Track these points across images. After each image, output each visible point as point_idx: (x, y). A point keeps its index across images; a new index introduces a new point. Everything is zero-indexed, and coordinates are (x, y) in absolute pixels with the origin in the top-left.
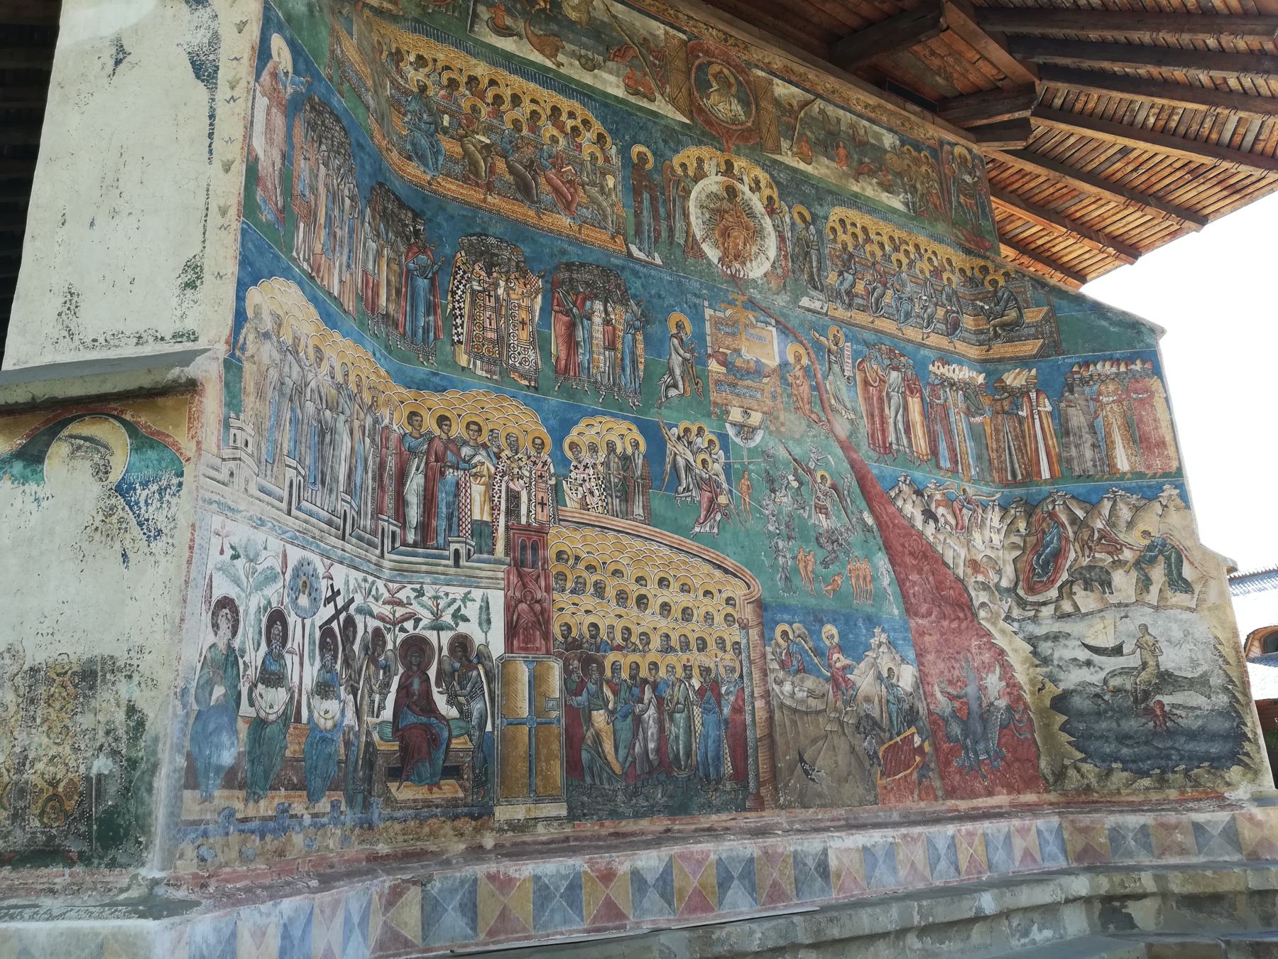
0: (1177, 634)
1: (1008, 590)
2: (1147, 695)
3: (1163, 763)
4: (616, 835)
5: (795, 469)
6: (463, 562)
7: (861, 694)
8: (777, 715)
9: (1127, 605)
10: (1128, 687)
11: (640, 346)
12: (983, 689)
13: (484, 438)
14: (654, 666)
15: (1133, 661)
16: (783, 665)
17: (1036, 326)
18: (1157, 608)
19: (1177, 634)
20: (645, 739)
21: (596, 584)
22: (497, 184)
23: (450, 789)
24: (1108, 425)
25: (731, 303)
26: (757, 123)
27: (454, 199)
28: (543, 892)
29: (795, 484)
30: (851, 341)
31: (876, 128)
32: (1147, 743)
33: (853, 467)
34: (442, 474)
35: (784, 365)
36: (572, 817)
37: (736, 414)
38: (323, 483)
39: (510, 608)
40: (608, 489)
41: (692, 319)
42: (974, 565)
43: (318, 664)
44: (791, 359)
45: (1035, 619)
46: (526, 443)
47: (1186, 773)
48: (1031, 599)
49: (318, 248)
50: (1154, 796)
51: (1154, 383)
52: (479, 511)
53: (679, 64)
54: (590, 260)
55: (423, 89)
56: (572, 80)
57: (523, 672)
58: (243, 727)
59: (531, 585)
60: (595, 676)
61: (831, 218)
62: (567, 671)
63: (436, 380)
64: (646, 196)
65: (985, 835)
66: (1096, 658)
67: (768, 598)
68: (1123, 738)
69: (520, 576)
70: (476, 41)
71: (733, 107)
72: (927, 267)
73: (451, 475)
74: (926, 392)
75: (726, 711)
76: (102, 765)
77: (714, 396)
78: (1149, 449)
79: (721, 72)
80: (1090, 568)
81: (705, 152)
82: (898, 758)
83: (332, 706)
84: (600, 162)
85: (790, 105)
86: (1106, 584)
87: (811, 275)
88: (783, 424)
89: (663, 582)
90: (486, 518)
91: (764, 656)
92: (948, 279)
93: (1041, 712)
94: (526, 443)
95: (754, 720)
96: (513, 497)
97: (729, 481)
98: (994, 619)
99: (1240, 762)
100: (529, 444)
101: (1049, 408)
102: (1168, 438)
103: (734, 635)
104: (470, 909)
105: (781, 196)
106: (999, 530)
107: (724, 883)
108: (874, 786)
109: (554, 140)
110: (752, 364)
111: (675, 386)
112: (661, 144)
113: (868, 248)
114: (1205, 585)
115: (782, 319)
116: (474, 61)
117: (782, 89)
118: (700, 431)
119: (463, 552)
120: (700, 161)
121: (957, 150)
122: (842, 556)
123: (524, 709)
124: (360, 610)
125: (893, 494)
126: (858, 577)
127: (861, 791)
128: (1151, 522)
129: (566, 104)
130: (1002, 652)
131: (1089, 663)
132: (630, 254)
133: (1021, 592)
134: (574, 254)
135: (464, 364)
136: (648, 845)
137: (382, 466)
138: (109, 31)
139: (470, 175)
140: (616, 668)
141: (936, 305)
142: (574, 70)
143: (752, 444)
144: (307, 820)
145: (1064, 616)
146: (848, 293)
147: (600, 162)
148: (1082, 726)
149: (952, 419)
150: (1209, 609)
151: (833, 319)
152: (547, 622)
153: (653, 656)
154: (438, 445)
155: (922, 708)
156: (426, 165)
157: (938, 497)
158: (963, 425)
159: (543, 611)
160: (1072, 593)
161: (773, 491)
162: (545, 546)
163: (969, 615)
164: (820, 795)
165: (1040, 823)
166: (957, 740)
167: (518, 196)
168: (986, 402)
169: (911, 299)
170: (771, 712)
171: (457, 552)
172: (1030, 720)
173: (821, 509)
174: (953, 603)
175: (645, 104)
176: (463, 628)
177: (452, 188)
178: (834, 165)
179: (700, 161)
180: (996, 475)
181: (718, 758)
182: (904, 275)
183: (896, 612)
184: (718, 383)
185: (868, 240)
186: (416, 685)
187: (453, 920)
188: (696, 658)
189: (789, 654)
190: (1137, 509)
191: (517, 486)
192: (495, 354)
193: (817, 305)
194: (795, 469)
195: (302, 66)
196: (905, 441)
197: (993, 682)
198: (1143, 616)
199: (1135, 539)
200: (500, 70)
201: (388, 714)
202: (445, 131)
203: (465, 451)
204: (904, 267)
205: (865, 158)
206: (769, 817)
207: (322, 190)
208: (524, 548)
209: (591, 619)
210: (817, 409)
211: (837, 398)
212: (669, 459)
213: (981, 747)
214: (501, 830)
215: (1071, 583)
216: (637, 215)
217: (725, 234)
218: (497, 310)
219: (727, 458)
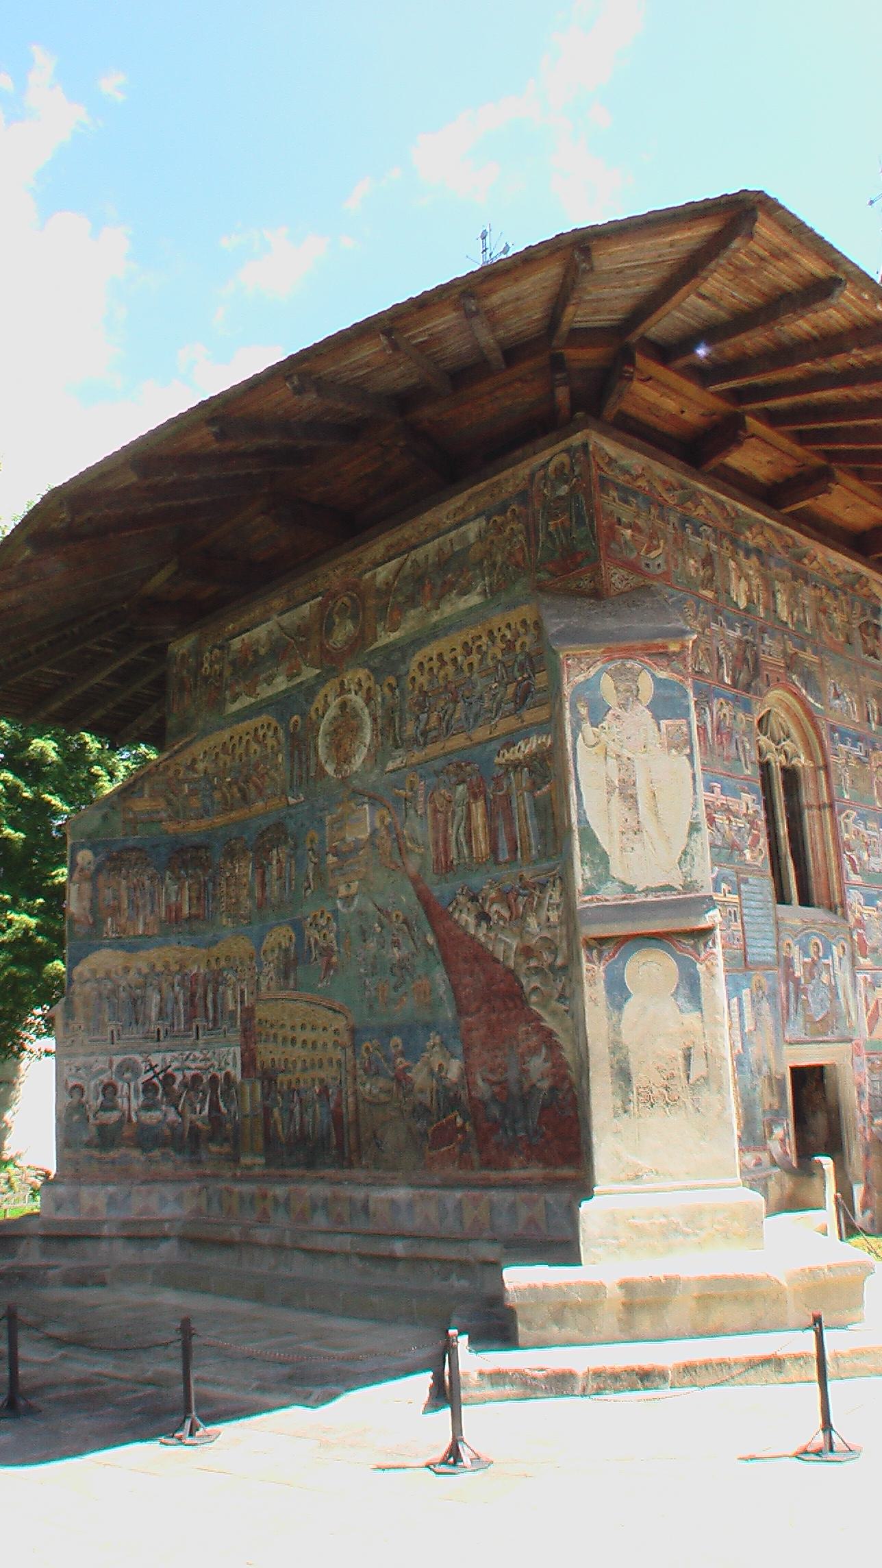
7: (417, 1086)
8: (361, 1107)
12: (524, 1072)
14: (298, 1080)
16: (365, 1070)
23: (226, 1148)
29: (379, 929)
37: (343, 891)
38: (137, 1023)
42: (527, 952)
43: (141, 1098)
44: (378, 824)
49: (123, 921)
52: (231, 1007)
57: (248, 1089)
62: (263, 1088)
65: (491, 1202)
73: (221, 988)
75: (332, 1105)
82: (443, 1136)
83: (156, 1115)
91: (355, 1066)
103: (338, 1054)
107: (314, 1208)
113: (442, 673)
117: (383, 574)
122: (408, 978)
124: (178, 1069)
130: (550, 1034)
137: (193, 995)
149: (515, 805)
153: (297, 1075)
155: (464, 1094)
157: (493, 894)
163: (519, 1003)
170: (357, 1105)
173: (396, 944)
177: (219, 820)
181: (329, 1134)
182: (475, 675)
185: (443, 663)
189: (370, 1063)
196: (466, 852)
197: (538, 1065)
201: (206, 1112)
207: (124, 893)
209: (271, 1056)
210: (396, 857)
211: (413, 840)
213: (519, 1125)
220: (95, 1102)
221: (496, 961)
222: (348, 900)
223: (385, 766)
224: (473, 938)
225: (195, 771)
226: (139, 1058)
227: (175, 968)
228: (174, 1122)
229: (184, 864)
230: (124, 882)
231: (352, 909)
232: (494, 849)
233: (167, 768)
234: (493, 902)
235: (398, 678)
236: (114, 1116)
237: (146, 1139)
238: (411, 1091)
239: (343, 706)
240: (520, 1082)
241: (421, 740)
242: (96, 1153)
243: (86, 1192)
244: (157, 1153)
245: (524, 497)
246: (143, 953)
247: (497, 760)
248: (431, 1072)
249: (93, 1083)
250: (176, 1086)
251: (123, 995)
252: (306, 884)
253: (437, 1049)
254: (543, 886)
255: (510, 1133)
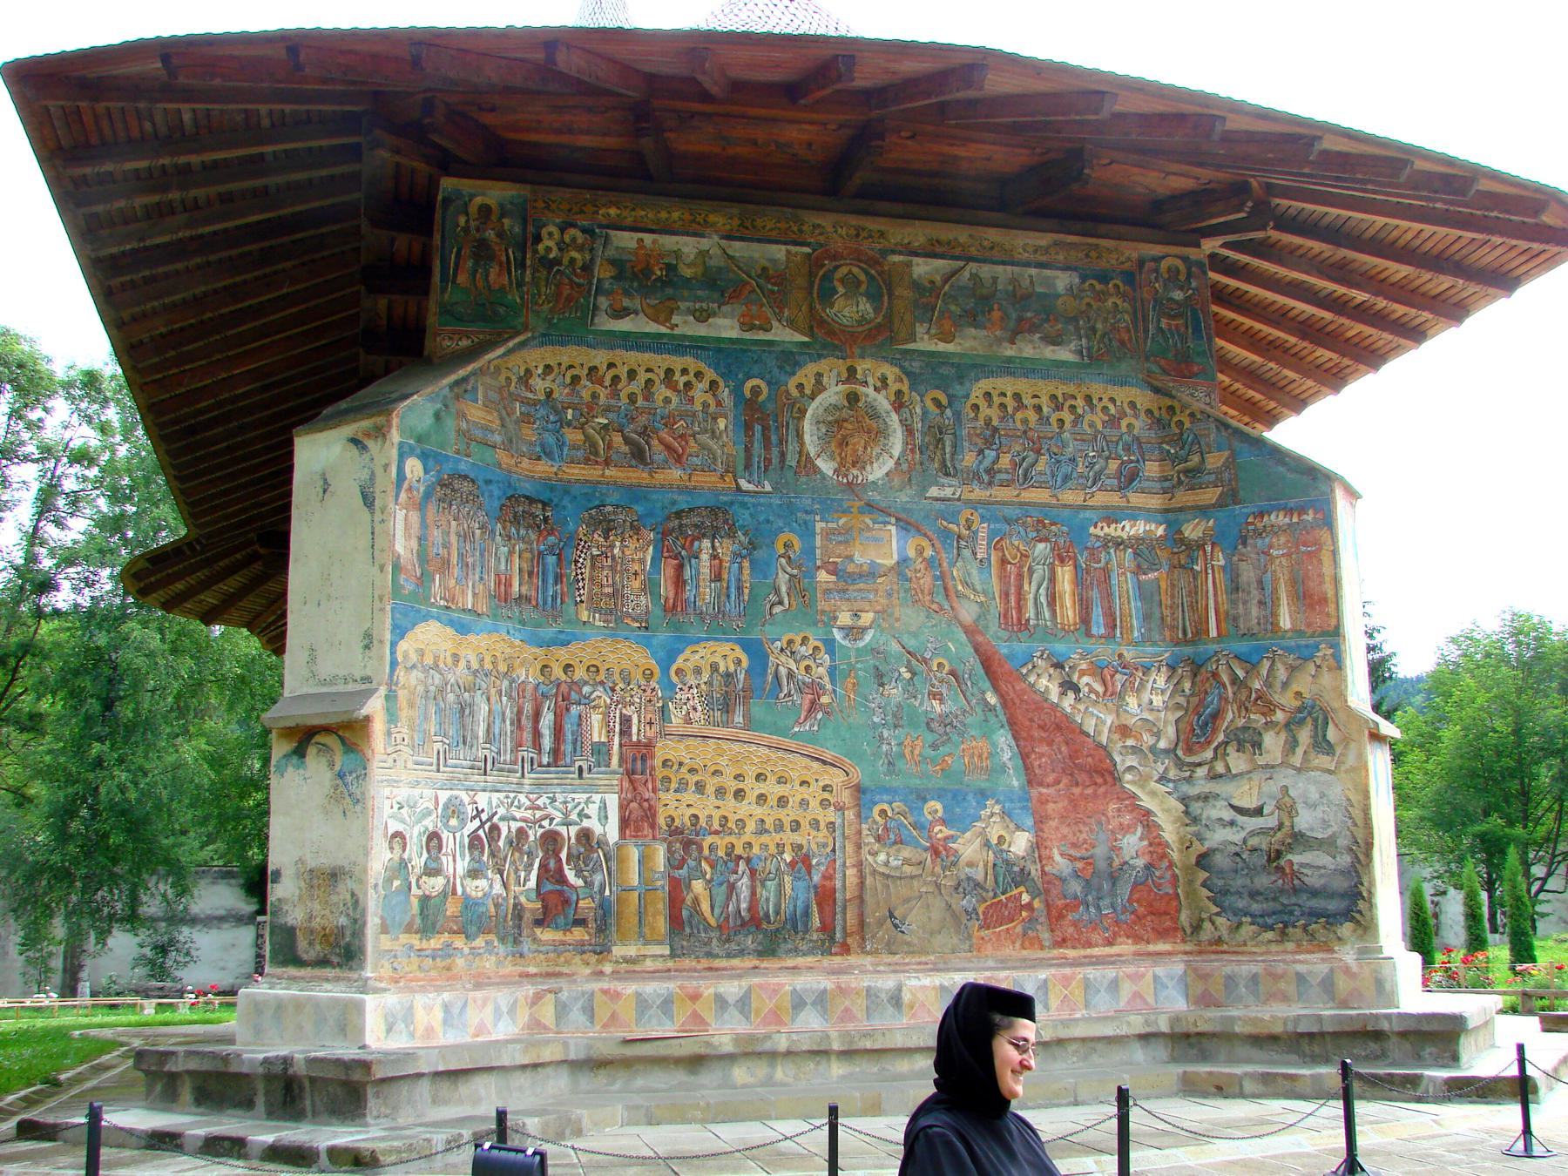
0: (1314, 796)
1: (1166, 751)
2: (1279, 854)
3: (1286, 918)
4: (710, 969)
5: (909, 661)
6: (585, 775)
8: (869, 881)
9: (1273, 767)
10: (1264, 847)
11: (746, 572)
13: (602, 677)
15: (1270, 822)
16: (878, 839)
17: (1218, 472)
18: (1299, 770)
19: (1314, 796)
20: (738, 901)
21: (697, 783)
22: (614, 457)
23: (578, 934)
24: (1275, 581)
25: (845, 512)
26: (889, 318)
27: (577, 481)
28: (642, 1003)
29: (907, 675)
30: (988, 521)
31: (1048, 272)
32: (1274, 899)
33: (976, 651)
34: (568, 710)
35: (904, 561)
36: (673, 955)
37: (845, 618)
39: (623, 807)
40: (709, 702)
41: (801, 537)
42: (1124, 731)
43: (468, 858)
44: (911, 553)
45: (1189, 780)
46: (637, 676)
47: (1305, 928)
48: (1188, 760)
49: (452, 583)
50: (1274, 948)
51: (1324, 535)
52: (598, 735)
53: (801, 281)
54: (699, 503)
55: (549, 394)
56: (684, 337)
57: (634, 854)
58: (415, 902)
59: (641, 789)
60: (695, 854)
61: (973, 396)
63: (562, 637)
64: (758, 428)
65: (1086, 979)
66: (1240, 819)
67: (867, 783)
68: (1254, 895)
69: (631, 781)
70: (595, 332)
71: (861, 307)
72: (1098, 419)
73: (574, 710)
74: (1081, 560)
75: (816, 878)
76: (343, 920)
77: (822, 605)
78: (1311, 606)
79: (850, 272)
80: (1245, 729)
81: (823, 365)
83: (482, 883)
84: (712, 408)
85: (932, 282)
86: (1257, 745)
87: (944, 460)
88: (898, 620)
89: (760, 777)
90: (603, 739)
91: (859, 832)
92: (1129, 425)
93: (1187, 869)
94: (637, 676)
95: (844, 886)
96: (626, 721)
97: (833, 681)
98: (1143, 781)
99: (1352, 919)
100: (639, 676)
101: (1222, 563)
102: (1330, 594)
104: (590, 1011)
105: (911, 388)
106: (1163, 692)
108: (970, 937)
109: (667, 401)
110: (865, 568)
111: (781, 603)
112: (776, 370)
113: (1019, 416)
114: (1346, 747)
115: (903, 516)
116: (594, 352)
117: (923, 268)
118: (805, 640)
119: (585, 767)
120: (819, 375)
121: (1164, 265)
122: (955, 737)
123: (634, 880)
124: (502, 819)
125: (1024, 671)
126: (972, 756)
127: (955, 940)
128: (1304, 684)
129: (677, 362)
130: (1148, 813)
131: (1232, 823)
132: (739, 489)
133: (1180, 753)
134: (683, 502)
135: (585, 619)
136: (732, 977)
137: (520, 713)
138: (318, 468)
139: (591, 454)
140: (712, 848)
141: (1108, 458)
142: (687, 326)
143: (861, 644)
144: (466, 950)
145: (1214, 777)
146: (989, 471)
147: (712, 408)
148: (1220, 883)
149: (1114, 582)
150: (1346, 771)
151: (968, 502)
152: (654, 816)
153: (746, 838)
154: (564, 688)
155: (1035, 871)
156: (553, 459)
157: (1084, 666)
158: (1130, 583)
159: (650, 808)
160: (1225, 754)
161: (882, 685)
162: (653, 757)
163: (1109, 779)
164: (908, 944)
165: (1160, 971)
166: (1076, 897)
167: (634, 463)
168: (1163, 555)
169: (1073, 460)
170: (862, 877)
171: (580, 768)
172: (1175, 876)
173: (935, 695)
174: (1094, 770)
175: (762, 336)
176: (586, 823)
177: (576, 472)
178: (985, 333)
179: (819, 375)
180: (1167, 633)
181: (807, 913)
182: (1066, 435)
183: (1016, 783)
184: (827, 591)
185: (1020, 406)
186: (552, 864)
187: (577, 1016)
188: (789, 837)
189: (886, 829)
190: (1292, 669)
191: (628, 711)
192: (612, 607)
193: (948, 492)
194: (909, 661)
195: (431, 463)
196: (1047, 615)
197: (1132, 844)
198: (1284, 778)
199: (1287, 700)
200: (618, 352)
201: (532, 883)
202: (569, 424)
203: (586, 689)
204: (1067, 426)
205: (1029, 314)
206: (852, 959)
208: (634, 760)
209: (692, 811)
210: (940, 598)
211: (966, 584)
212: (771, 670)
213: (1106, 902)
214: (617, 962)
215: (1227, 743)
216: (747, 450)
217: (843, 443)
218: (612, 568)
219: (832, 660)
220: (418, 861)
221: (1088, 735)
222: (854, 632)
223: (925, 489)
224: (1055, 707)
225: (529, 388)
226: (466, 799)
227: (503, 668)
228: (499, 896)
229: (516, 521)
230: (454, 523)
231: (861, 644)
232: (1085, 620)
233: (498, 369)
234: (1083, 673)
235: (952, 398)
236: (439, 882)
237: (473, 921)
238: (954, 864)
239: (853, 398)
240: (1110, 860)
241: (986, 478)
242: (415, 940)
243: (420, 1000)
244: (479, 942)
245: (1129, 277)
246: (471, 637)
247: (1092, 530)
248: (987, 844)
249: (416, 833)
250: (501, 843)
251: (451, 697)
252: (773, 598)
253: (996, 819)
254: (1146, 670)
255: (1092, 910)
